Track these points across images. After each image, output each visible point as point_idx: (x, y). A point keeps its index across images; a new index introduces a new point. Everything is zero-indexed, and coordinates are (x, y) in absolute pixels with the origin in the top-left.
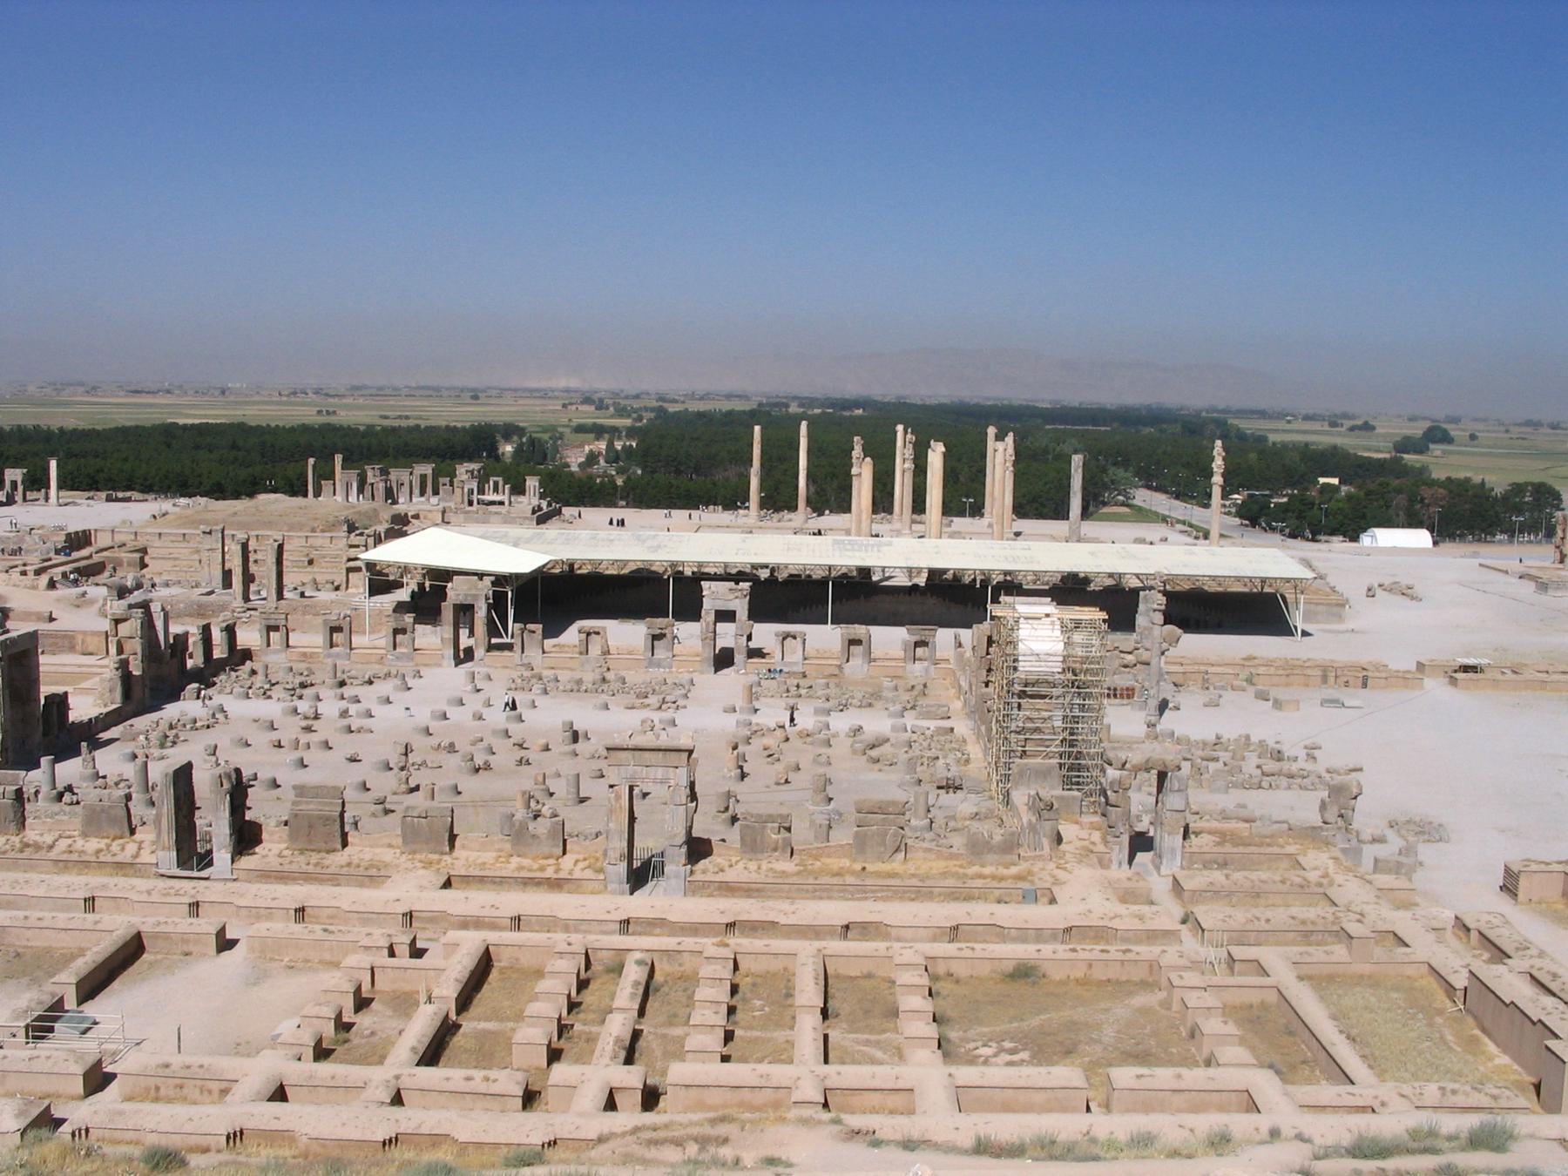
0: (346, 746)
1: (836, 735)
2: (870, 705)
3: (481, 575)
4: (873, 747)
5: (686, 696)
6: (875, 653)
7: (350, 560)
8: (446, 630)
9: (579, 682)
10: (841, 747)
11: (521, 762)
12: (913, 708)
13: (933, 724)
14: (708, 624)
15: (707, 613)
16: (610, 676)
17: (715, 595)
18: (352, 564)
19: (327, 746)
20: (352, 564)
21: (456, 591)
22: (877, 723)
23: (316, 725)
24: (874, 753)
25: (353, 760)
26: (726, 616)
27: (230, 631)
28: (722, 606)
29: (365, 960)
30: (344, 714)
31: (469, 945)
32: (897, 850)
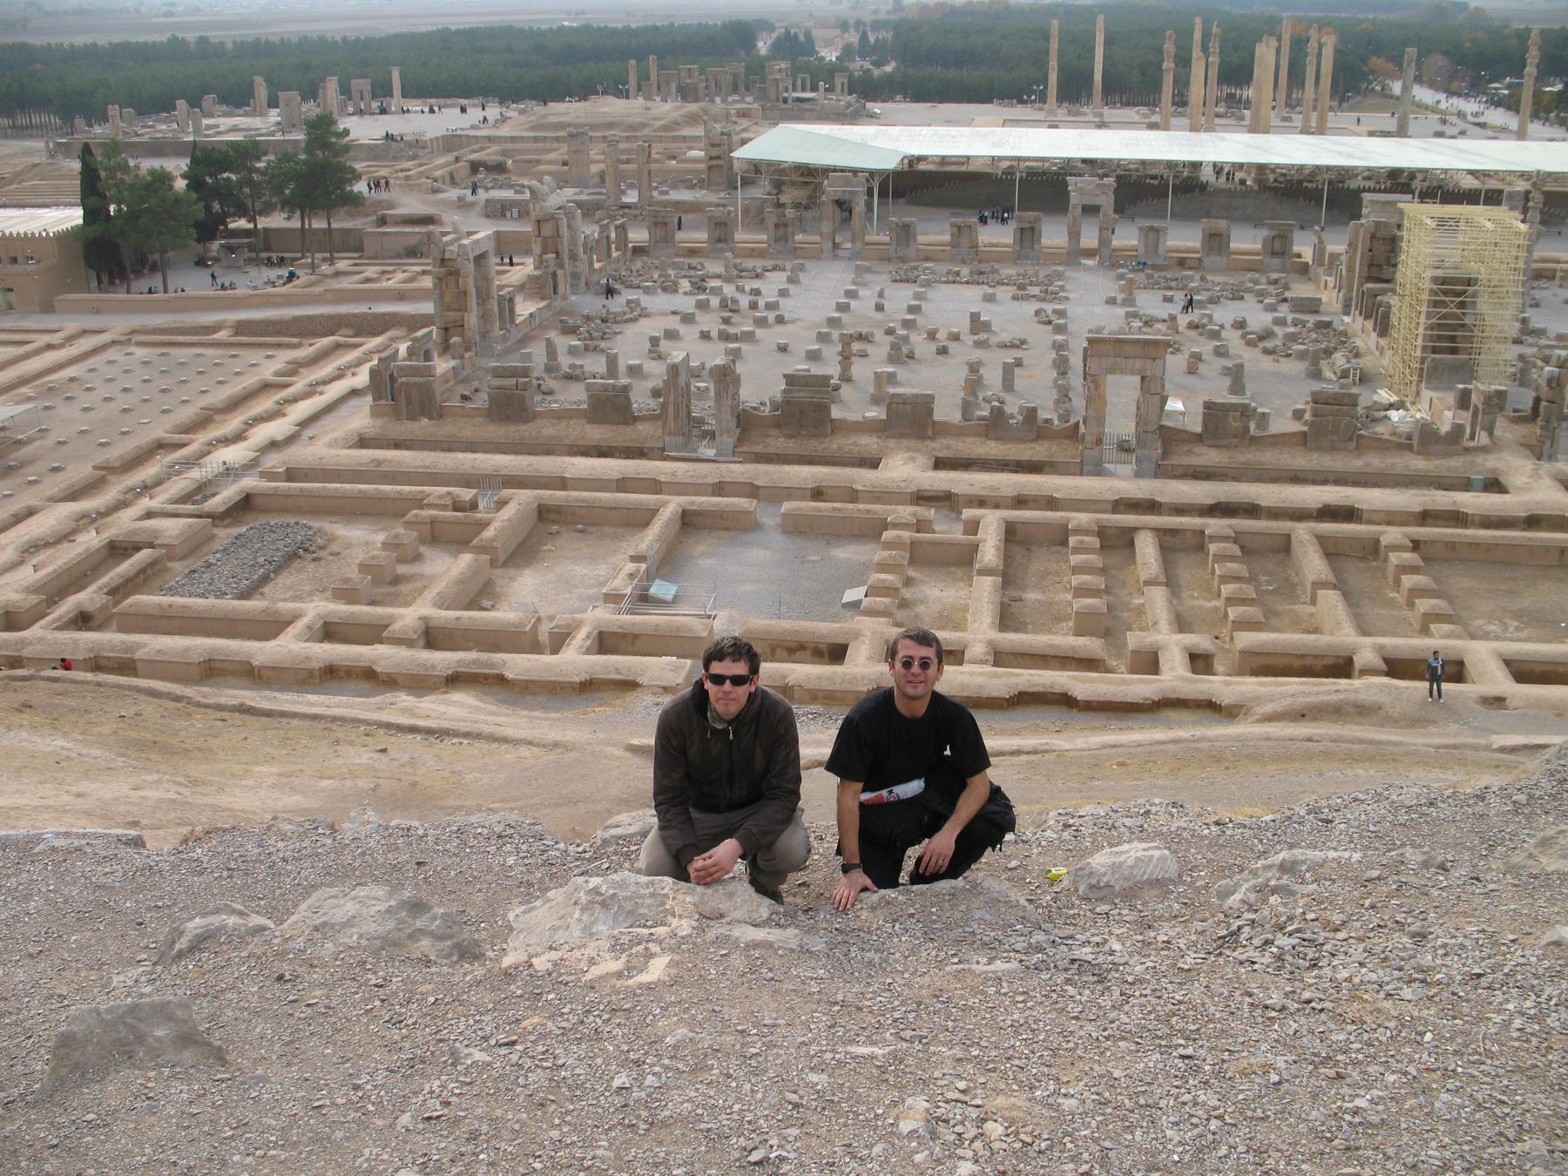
0: (771, 337)
1: (1222, 326)
2: (1242, 298)
3: (855, 171)
4: (1261, 338)
5: (1062, 288)
6: (1232, 245)
7: (711, 158)
8: (826, 227)
9: (958, 274)
10: (1232, 338)
11: (943, 351)
12: (1285, 300)
13: (1311, 320)
14: (1075, 218)
15: (1074, 208)
16: (985, 267)
17: (1080, 189)
18: (714, 163)
19: (749, 337)
20: (714, 163)
21: (832, 189)
22: (1259, 319)
23: (735, 318)
24: (1269, 344)
25: (783, 349)
26: (1091, 210)
27: (622, 229)
28: (1089, 201)
29: (906, 535)
30: (753, 306)
31: (991, 524)
32: (1350, 439)
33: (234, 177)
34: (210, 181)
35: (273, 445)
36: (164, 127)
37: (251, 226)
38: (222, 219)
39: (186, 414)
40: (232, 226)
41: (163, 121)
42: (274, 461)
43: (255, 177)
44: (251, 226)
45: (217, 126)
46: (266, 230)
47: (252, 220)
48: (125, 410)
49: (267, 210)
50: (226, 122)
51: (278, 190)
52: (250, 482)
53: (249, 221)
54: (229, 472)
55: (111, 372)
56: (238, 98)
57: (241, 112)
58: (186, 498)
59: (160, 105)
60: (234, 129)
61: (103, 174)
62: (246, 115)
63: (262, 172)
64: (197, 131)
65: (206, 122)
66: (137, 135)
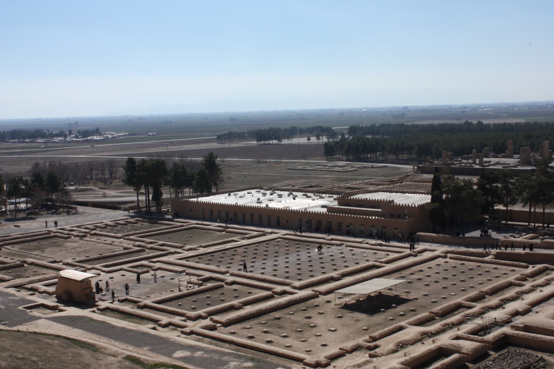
33: (499, 185)
34: (488, 186)
35: (516, 313)
36: (465, 161)
37: (505, 208)
38: (492, 204)
39: (473, 293)
40: (496, 208)
41: (465, 159)
42: (519, 321)
43: (511, 186)
44: (505, 208)
45: (490, 162)
46: (510, 210)
47: (506, 205)
48: (444, 288)
49: (514, 202)
50: (494, 160)
51: (521, 194)
52: (506, 330)
53: (504, 206)
54: (496, 324)
55: (440, 269)
56: (499, 150)
57: (501, 156)
58: (475, 332)
59: (464, 152)
60: (498, 163)
61: (442, 180)
62: (503, 157)
63: (513, 184)
64: (481, 164)
65: (485, 159)
66: (453, 164)
